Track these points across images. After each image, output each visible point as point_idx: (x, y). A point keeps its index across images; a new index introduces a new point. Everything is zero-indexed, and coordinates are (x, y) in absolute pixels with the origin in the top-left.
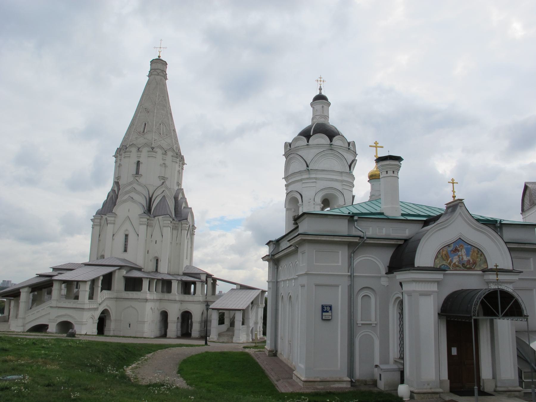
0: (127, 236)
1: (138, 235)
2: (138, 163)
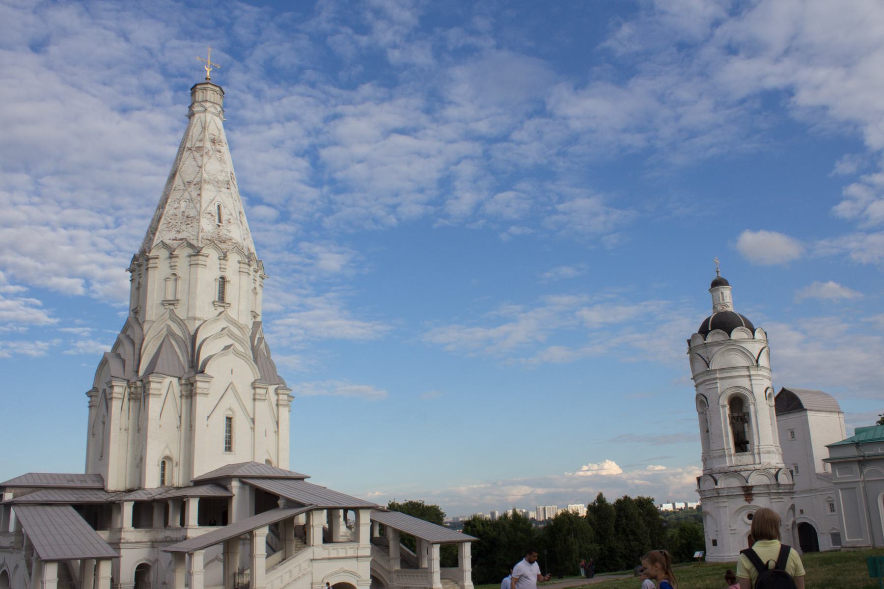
0: (229, 419)
1: (253, 421)
2: (223, 281)
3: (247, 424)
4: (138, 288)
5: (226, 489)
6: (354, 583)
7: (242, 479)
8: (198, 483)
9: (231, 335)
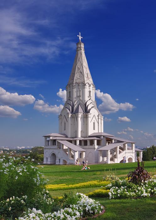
0: (94, 123)
1: (98, 123)
2: (90, 92)
3: (97, 124)
4: (70, 92)
5: (100, 138)
6: (132, 157)
7: (103, 136)
8: (90, 137)
9: (93, 104)
